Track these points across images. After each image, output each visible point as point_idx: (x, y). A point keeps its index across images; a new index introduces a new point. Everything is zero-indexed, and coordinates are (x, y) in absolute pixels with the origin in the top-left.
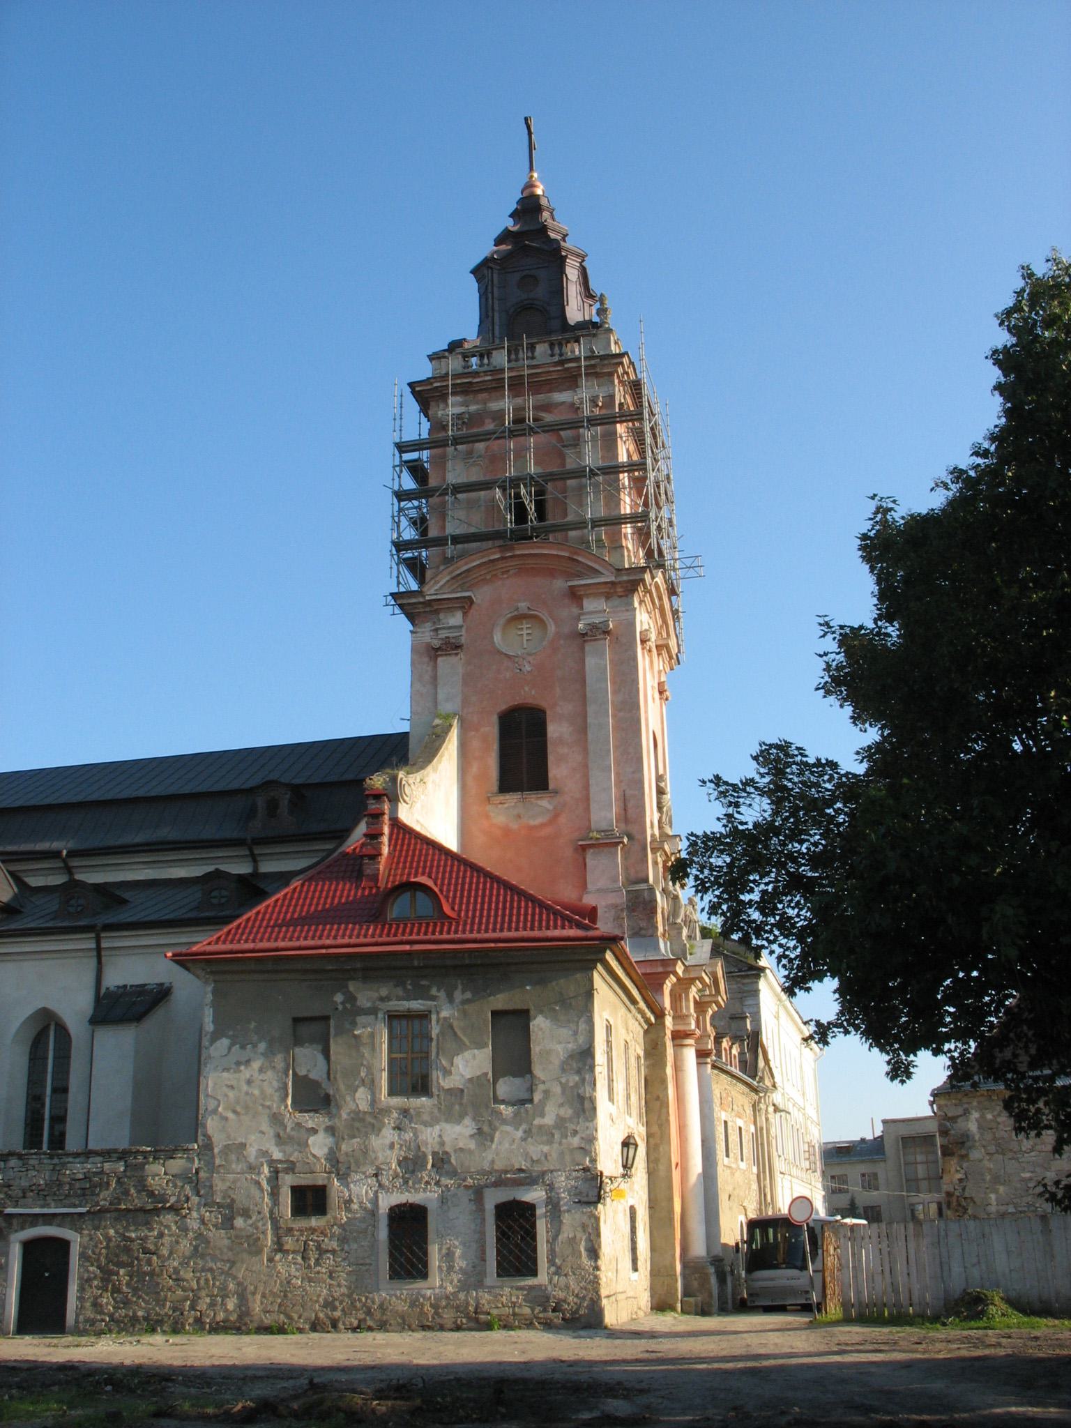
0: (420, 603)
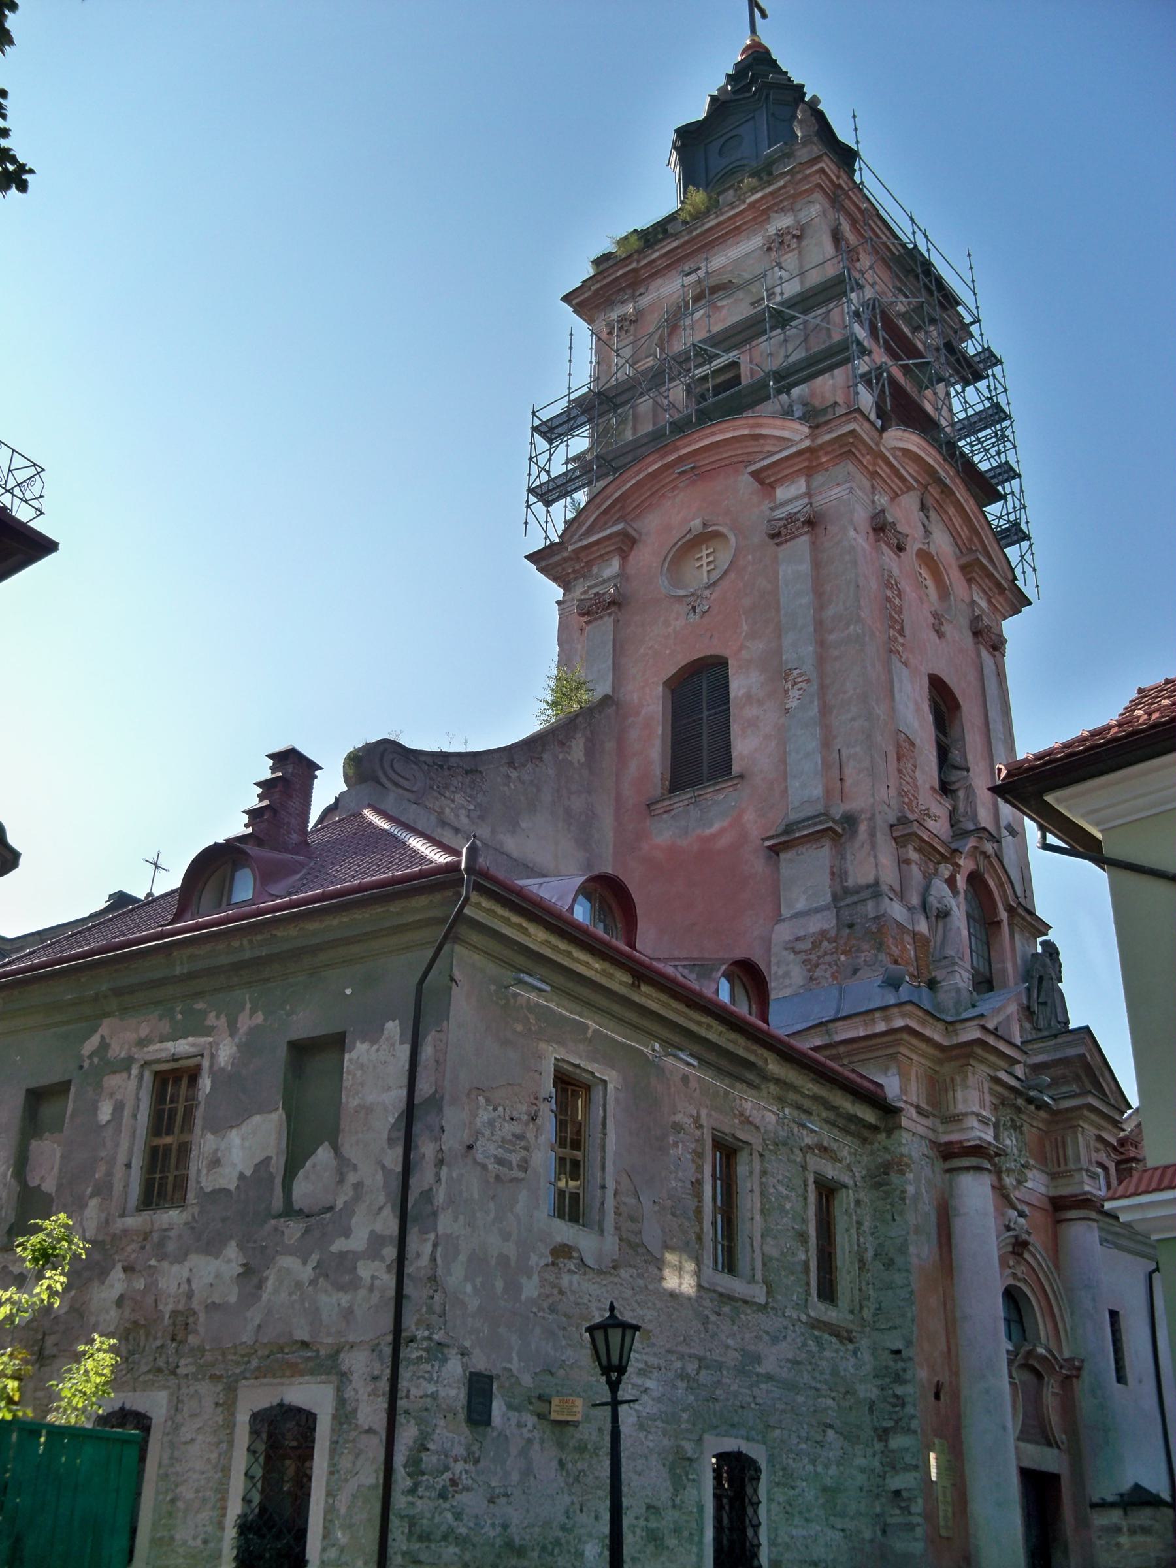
0: (565, 560)
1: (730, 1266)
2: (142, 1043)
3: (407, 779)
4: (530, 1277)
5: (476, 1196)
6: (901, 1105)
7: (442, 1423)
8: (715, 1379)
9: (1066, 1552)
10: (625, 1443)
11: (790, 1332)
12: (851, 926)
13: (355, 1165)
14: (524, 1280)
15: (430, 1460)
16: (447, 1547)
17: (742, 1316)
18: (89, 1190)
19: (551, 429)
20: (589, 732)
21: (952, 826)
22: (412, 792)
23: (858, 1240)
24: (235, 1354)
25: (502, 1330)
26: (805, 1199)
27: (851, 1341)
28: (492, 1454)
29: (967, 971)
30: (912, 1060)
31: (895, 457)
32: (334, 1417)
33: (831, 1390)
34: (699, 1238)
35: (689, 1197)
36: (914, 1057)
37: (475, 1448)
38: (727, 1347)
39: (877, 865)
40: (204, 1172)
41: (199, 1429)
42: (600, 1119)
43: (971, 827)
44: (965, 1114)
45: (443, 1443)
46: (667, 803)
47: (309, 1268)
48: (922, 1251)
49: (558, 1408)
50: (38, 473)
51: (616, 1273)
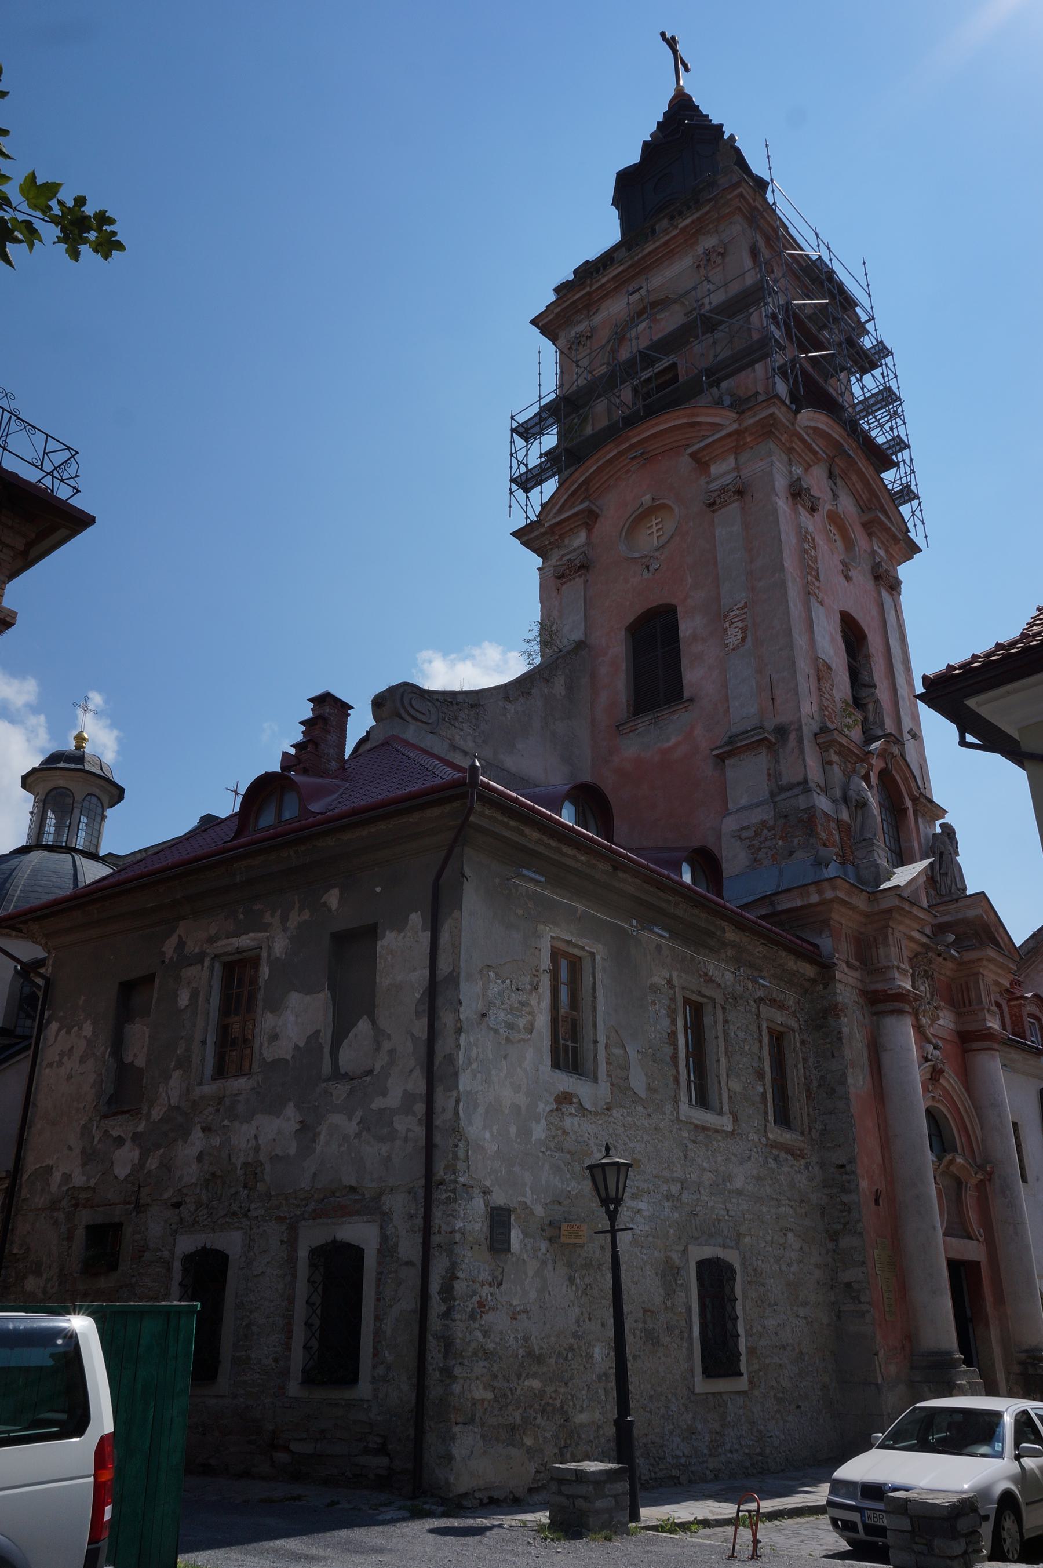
0: (543, 534)
1: (703, 1101)
2: (211, 940)
3: (424, 714)
4: (538, 1122)
5: (491, 1056)
6: (836, 961)
7: (469, 1254)
8: (695, 1197)
9: (987, 1325)
10: (623, 1259)
11: (753, 1153)
12: (786, 816)
13: (389, 1035)
14: (533, 1125)
15: (460, 1287)
16: (477, 1362)
17: (714, 1142)
18: (173, 1064)
19: (527, 430)
20: (567, 671)
21: (864, 733)
22: (428, 723)
23: (805, 1073)
24: (296, 1198)
25: (517, 1169)
26: (760, 1042)
27: (803, 1158)
28: (512, 1276)
29: (883, 850)
30: (842, 924)
31: (808, 435)
32: (379, 1251)
33: (790, 1200)
34: (677, 1080)
35: (666, 1046)
36: (843, 922)
37: (498, 1273)
38: (704, 1170)
39: (805, 766)
40: (266, 1044)
41: (268, 1263)
42: (591, 986)
43: (881, 733)
44: (889, 967)
45: (471, 1271)
46: (633, 724)
47: (354, 1123)
48: (858, 1082)
49: (566, 1233)
50: (73, 456)
51: (609, 1113)
